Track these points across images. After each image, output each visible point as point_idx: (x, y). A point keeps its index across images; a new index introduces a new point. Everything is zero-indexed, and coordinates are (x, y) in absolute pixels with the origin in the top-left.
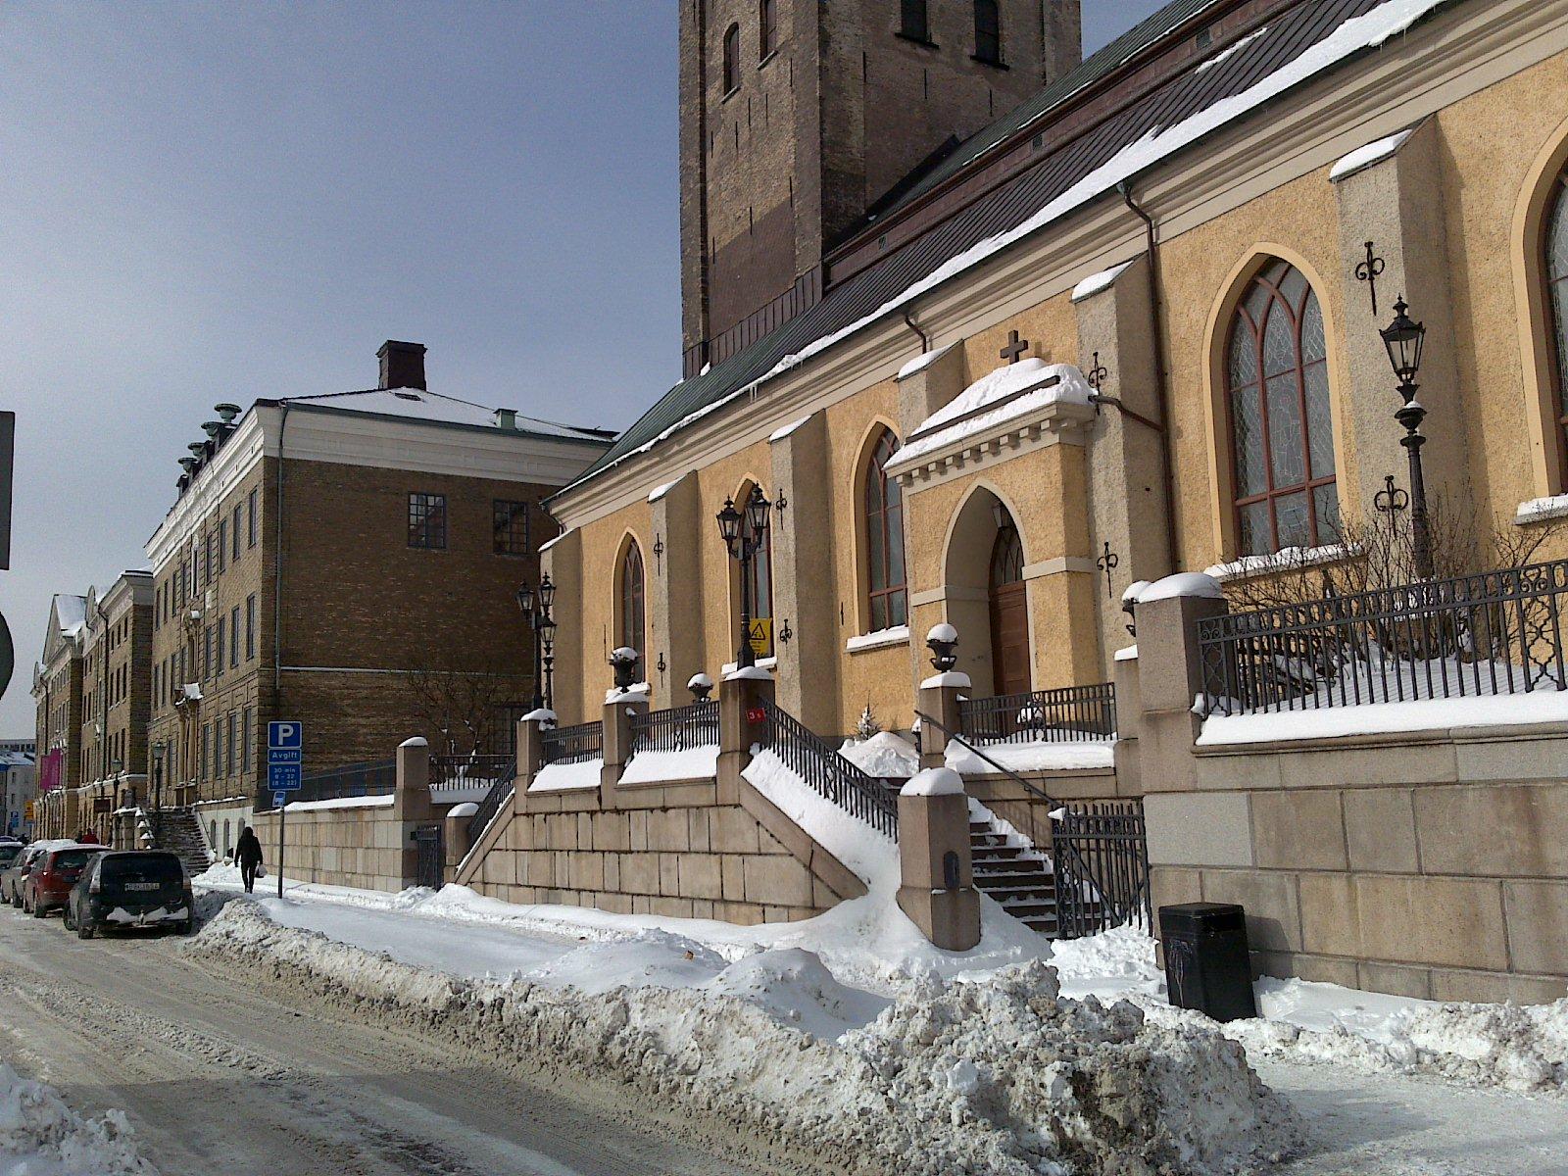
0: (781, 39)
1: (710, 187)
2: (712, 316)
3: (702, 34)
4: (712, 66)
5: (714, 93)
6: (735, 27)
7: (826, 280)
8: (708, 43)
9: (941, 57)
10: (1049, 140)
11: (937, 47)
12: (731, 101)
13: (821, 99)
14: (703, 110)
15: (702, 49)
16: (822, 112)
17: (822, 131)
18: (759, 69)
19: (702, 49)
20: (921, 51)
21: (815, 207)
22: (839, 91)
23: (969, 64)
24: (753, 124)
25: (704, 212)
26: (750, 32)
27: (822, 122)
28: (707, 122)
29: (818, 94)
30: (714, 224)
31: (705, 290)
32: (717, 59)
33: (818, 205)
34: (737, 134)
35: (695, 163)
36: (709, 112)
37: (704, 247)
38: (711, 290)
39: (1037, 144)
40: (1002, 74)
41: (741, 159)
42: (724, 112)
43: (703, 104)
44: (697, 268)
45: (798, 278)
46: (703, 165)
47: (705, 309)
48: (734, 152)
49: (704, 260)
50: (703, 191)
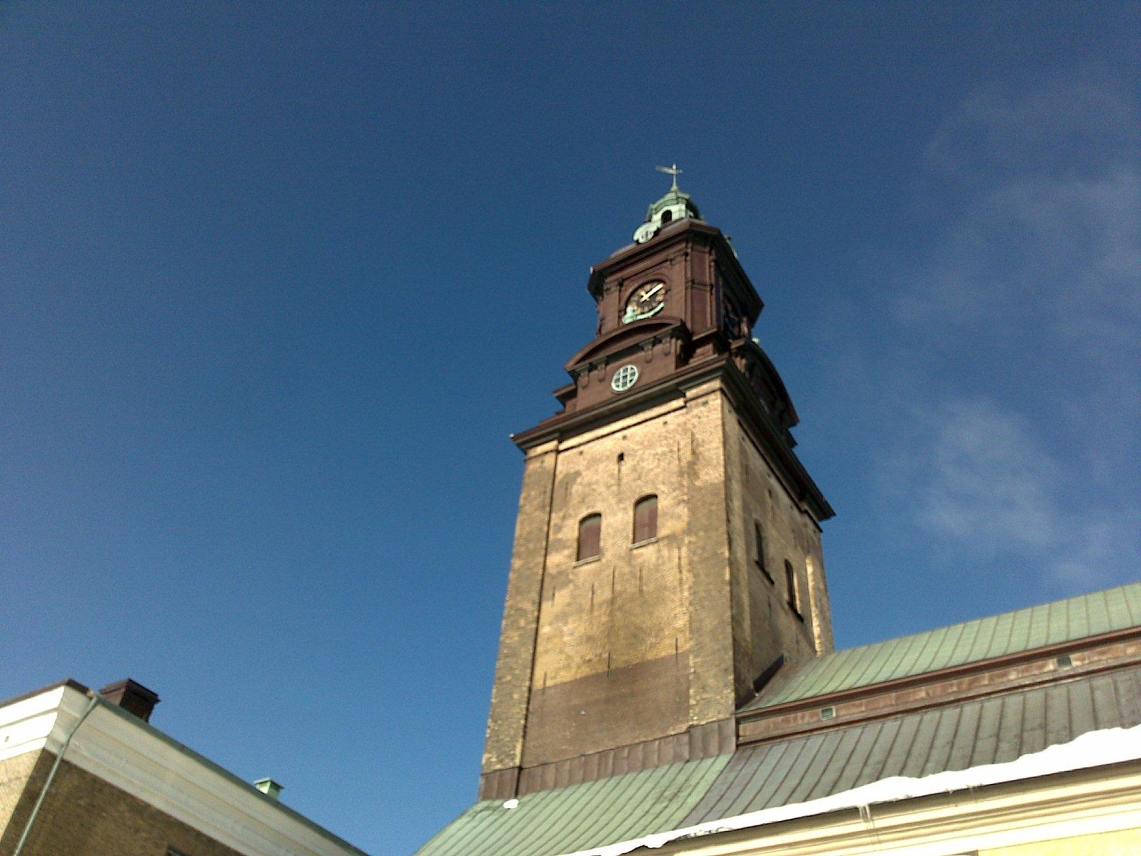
0: (663, 532)
1: (545, 630)
2: (530, 744)
3: (550, 513)
4: (559, 541)
6: (598, 515)
7: (738, 736)
10: (1077, 662)
11: (772, 582)
13: (731, 583)
16: (731, 592)
17: (732, 607)
18: (632, 550)
21: (723, 666)
22: (738, 583)
23: (787, 607)
24: (618, 588)
25: (535, 648)
26: (617, 521)
27: (731, 600)
28: (547, 580)
29: (727, 577)
31: (526, 718)
32: (570, 531)
33: (729, 662)
34: (593, 594)
37: (531, 679)
39: (1065, 661)
40: (800, 622)
42: (575, 575)
43: (545, 562)
45: (692, 727)
46: (539, 610)
47: (524, 737)
48: (587, 607)
49: (530, 690)
50: (537, 630)
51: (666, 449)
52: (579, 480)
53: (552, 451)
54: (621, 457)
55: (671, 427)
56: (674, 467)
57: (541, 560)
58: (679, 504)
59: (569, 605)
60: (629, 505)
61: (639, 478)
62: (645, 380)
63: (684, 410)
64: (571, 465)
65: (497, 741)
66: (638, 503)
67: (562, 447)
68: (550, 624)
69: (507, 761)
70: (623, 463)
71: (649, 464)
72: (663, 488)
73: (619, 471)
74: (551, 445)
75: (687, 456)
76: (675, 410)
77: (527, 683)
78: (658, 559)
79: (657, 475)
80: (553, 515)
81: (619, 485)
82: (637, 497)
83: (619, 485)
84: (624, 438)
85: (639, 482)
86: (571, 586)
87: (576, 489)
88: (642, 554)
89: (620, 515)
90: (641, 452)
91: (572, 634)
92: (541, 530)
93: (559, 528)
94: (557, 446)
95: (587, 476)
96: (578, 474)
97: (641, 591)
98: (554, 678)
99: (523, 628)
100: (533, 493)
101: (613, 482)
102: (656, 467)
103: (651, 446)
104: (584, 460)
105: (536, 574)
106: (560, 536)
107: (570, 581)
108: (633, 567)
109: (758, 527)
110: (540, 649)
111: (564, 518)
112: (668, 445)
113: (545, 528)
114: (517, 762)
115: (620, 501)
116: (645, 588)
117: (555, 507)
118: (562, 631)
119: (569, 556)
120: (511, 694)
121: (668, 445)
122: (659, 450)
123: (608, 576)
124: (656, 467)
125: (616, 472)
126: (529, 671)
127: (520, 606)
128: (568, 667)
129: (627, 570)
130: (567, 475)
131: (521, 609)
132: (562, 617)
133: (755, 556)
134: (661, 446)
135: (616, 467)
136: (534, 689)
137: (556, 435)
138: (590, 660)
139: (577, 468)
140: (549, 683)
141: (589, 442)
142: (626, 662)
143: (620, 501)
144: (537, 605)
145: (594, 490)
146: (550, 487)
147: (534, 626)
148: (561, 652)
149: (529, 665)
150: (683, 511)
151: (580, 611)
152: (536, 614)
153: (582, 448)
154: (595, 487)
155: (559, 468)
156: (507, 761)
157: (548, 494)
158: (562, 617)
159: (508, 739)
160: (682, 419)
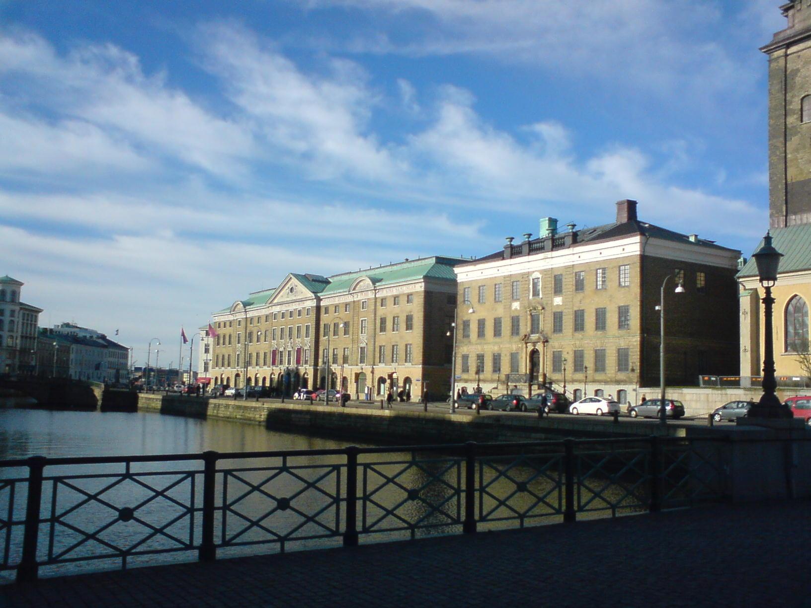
1: (789, 156)
4: (791, 110)
5: (792, 120)
8: (788, 98)
12: (805, 125)
15: (785, 100)
19: (785, 100)
30: (791, 172)
31: (786, 196)
35: (782, 146)
36: (789, 126)
37: (786, 178)
38: (789, 196)
43: (785, 122)
44: (781, 186)
47: (786, 203)
52: (799, 74)
53: (782, 56)
59: (799, 144)
64: (794, 64)
65: (775, 205)
67: (789, 51)
68: (791, 153)
74: (781, 52)
77: (784, 181)
80: (787, 95)
86: (799, 135)
87: (798, 80)
91: (802, 159)
92: (781, 104)
93: (791, 103)
94: (786, 52)
95: (803, 72)
96: (798, 70)
98: (795, 178)
99: (779, 156)
100: (775, 82)
104: (801, 61)
105: (782, 129)
107: (799, 132)
110: (788, 164)
111: (793, 97)
113: (784, 103)
114: (784, 213)
117: (788, 91)
118: (797, 157)
119: (796, 119)
127: (776, 144)
130: (792, 71)
132: (797, 150)
136: (788, 183)
137: (785, 46)
140: (793, 181)
141: (803, 50)
144: (784, 143)
145: (808, 81)
147: (784, 155)
148: (797, 168)
153: (800, 53)
155: (788, 66)
158: (797, 150)
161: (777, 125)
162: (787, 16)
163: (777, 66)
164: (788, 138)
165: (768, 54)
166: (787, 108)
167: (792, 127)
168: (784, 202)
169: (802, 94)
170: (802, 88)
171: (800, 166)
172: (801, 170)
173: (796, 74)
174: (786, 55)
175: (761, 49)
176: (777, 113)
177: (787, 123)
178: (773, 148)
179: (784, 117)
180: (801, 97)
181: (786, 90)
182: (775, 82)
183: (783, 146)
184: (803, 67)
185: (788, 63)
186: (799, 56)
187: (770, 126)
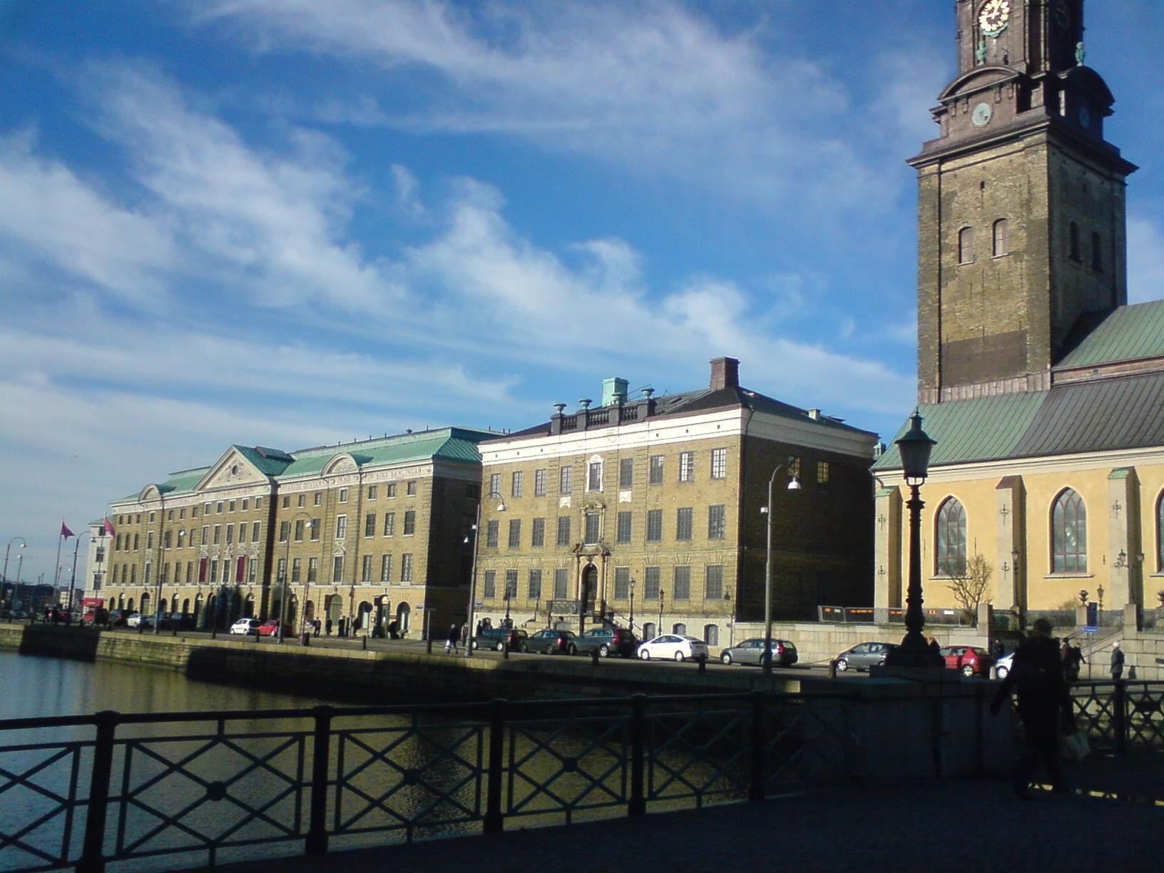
1: (944, 307)
4: (947, 244)
5: (948, 258)
9: (1083, 267)
14: (940, 265)
15: (940, 233)
20: (1077, 265)
25: (940, 319)
31: (940, 361)
36: (944, 267)
41: (974, 300)
43: (940, 261)
46: (940, 294)
48: (968, 295)
49: (940, 344)
50: (940, 307)
51: (1011, 184)
52: (956, 199)
54: (982, 185)
55: (1015, 165)
56: (1017, 200)
57: (938, 259)
58: (1020, 230)
59: (957, 292)
60: (990, 223)
61: (995, 205)
62: (997, 124)
63: (1023, 152)
66: (995, 224)
69: (931, 384)
70: (984, 190)
71: (1001, 194)
72: (1010, 215)
73: (982, 196)
75: (1025, 196)
76: (1016, 152)
77: (937, 341)
78: (1009, 266)
79: (1006, 203)
80: (942, 225)
81: (982, 207)
82: (995, 219)
83: (982, 207)
84: (984, 168)
85: (995, 208)
86: (957, 279)
87: (954, 205)
88: (999, 263)
89: (984, 233)
90: (995, 183)
91: (960, 312)
96: (954, 194)
97: (999, 289)
101: (978, 205)
102: (1007, 197)
103: (1001, 179)
106: (947, 242)
107: (957, 276)
108: (995, 271)
109: (1073, 225)
110: (942, 318)
112: (1013, 181)
113: (937, 236)
114: (937, 385)
115: (984, 221)
116: (1001, 287)
117: (943, 219)
119: (954, 258)
120: (929, 346)
121: (1013, 181)
122: (1008, 184)
123: (979, 275)
124: (1007, 197)
125: (980, 197)
126: (937, 333)
127: (927, 290)
128: (959, 332)
129: (990, 273)
131: (928, 292)
132: (954, 300)
133: (1069, 253)
134: (1008, 180)
135: (979, 192)
137: (938, 161)
138: (972, 329)
139: (954, 189)
140: (949, 341)
141: (960, 168)
142: (992, 332)
143: (984, 221)
144: (938, 290)
145: (966, 208)
146: (937, 203)
148: (955, 323)
149: (937, 329)
150: (1023, 234)
151: (963, 297)
152: (938, 297)
154: (967, 206)
156: (931, 384)
157: (937, 209)
158: (954, 300)
159: (930, 372)
160: (1021, 160)
161: (928, 264)
162: (939, 122)
163: (928, 185)
164: (942, 284)
165: (917, 168)
166: (942, 241)
167: (949, 268)
168: (937, 369)
169: (960, 225)
170: (960, 218)
171: (959, 321)
172: (960, 327)
173: (953, 198)
174: (940, 173)
175: (908, 161)
176: (929, 248)
177: (942, 262)
178: (923, 295)
179: (938, 253)
180: (959, 229)
181: (940, 218)
182: (926, 206)
183: (936, 293)
184: (961, 190)
185: (942, 182)
186: (956, 175)
187: (919, 264)
